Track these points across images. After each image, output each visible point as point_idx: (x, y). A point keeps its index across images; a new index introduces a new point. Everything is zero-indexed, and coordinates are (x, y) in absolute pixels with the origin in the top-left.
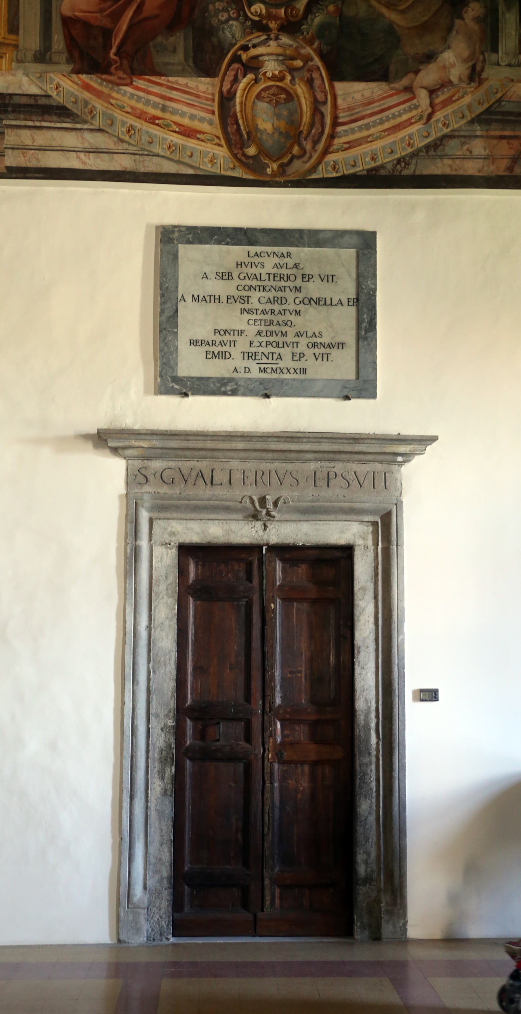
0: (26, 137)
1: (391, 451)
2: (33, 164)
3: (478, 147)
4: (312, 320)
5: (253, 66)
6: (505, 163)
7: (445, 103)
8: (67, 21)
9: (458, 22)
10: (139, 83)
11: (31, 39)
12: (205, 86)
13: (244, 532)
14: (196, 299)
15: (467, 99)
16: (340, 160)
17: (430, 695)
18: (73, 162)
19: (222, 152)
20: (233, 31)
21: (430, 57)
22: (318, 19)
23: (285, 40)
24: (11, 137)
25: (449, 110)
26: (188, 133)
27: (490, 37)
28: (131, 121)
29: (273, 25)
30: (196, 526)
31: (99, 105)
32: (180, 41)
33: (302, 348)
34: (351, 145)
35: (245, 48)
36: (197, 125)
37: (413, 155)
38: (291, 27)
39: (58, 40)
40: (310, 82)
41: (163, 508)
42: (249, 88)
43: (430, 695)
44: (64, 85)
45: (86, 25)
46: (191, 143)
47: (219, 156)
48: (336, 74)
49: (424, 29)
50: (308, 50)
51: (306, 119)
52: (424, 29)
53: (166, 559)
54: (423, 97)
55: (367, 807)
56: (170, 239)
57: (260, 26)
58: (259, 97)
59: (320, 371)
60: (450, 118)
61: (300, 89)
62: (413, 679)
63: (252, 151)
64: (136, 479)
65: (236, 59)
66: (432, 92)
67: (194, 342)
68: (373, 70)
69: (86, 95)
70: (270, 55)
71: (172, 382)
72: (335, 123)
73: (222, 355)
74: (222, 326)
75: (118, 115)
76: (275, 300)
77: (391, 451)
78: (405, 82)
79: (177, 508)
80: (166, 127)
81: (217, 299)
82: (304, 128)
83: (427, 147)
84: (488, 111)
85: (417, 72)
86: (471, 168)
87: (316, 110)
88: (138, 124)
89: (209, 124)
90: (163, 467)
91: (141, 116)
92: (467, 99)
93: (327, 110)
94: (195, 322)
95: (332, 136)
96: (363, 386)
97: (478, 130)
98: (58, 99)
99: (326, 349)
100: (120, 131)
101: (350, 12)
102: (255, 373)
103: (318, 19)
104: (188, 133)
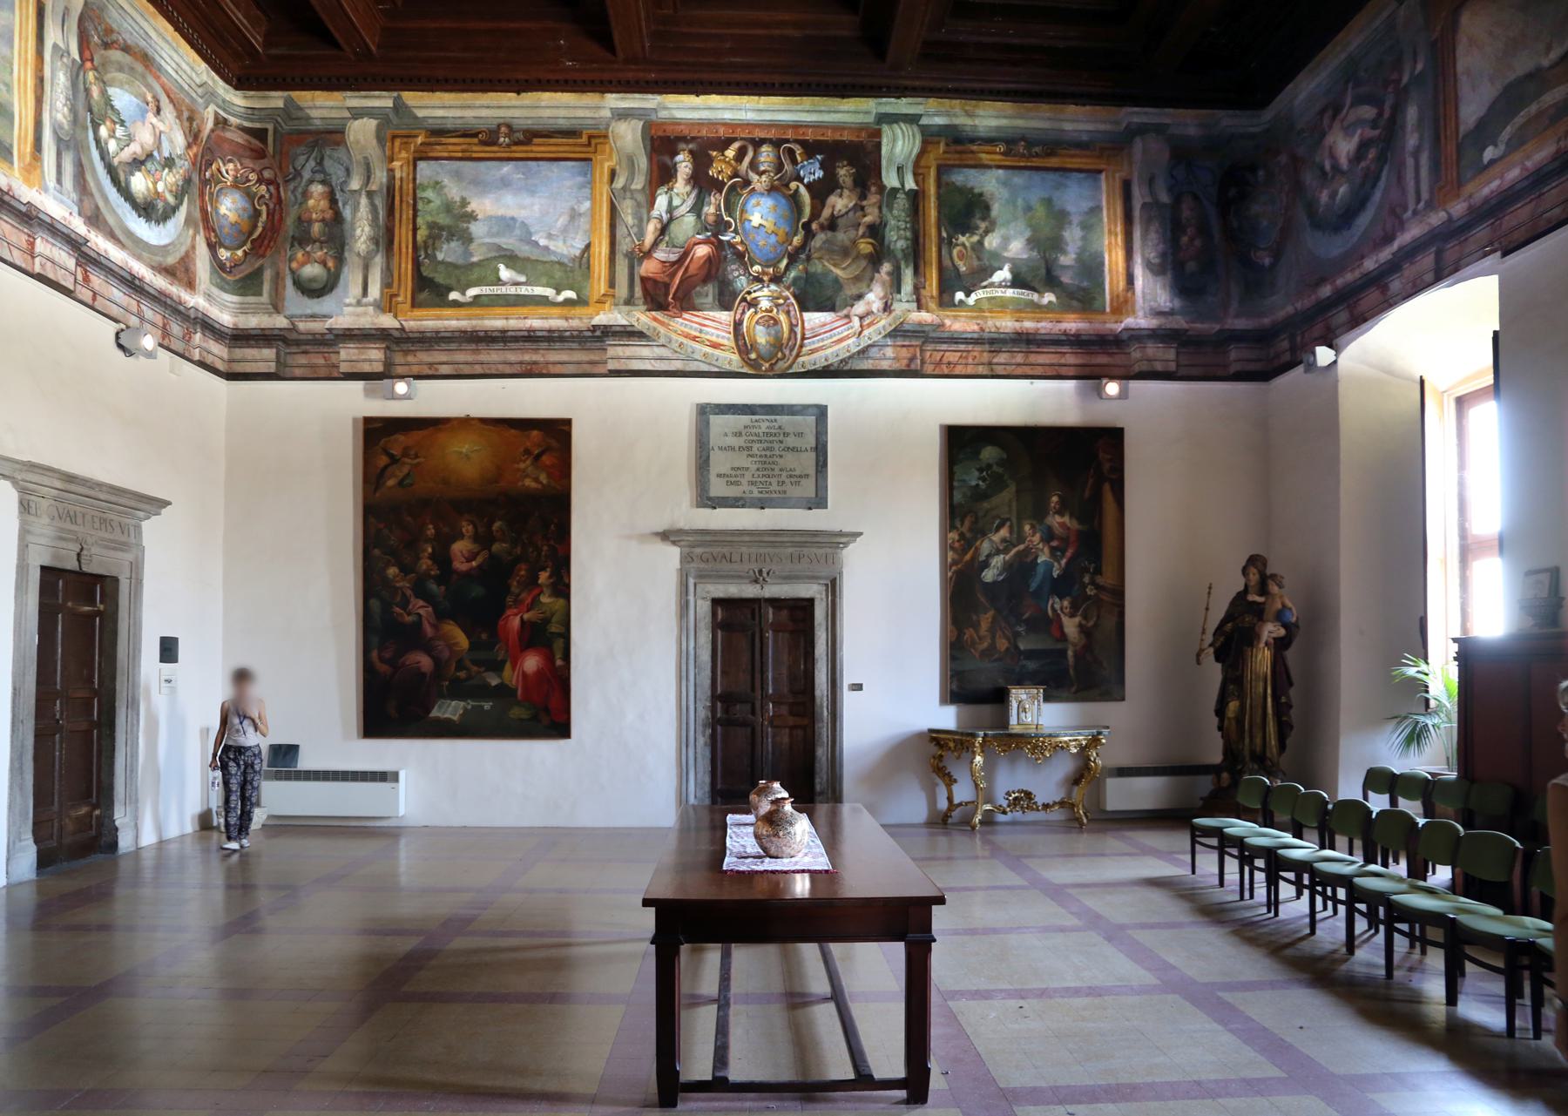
0: (620, 351)
1: (835, 541)
2: (623, 367)
3: (889, 352)
4: (789, 460)
5: (753, 304)
6: (905, 362)
7: (869, 325)
8: (644, 280)
10: (685, 315)
11: (622, 290)
12: (726, 317)
13: (750, 591)
14: (720, 448)
15: (883, 322)
16: (807, 361)
18: (647, 366)
19: (736, 357)
20: (742, 282)
21: (860, 297)
22: (793, 274)
23: (773, 287)
24: (611, 352)
25: (871, 329)
26: (715, 346)
27: (896, 284)
30: (721, 587)
31: (662, 330)
32: (710, 289)
33: (783, 478)
34: (813, 351)
38: (776, 279)
40: (788, 313)
41: (702, 576)
42: (752, 317)
44: (641, 318)
45: (655, 281)
46: (717, 352)
47: (732, 360)
49: (857, 279)
50: (787, 293)
51: (786, 335)
52: (857, 279)
54: (856, 321)
57: (758, 279)
59: (794, 492)
60: (872, 334)
61: (782, 317)
63: (753, 356)
64: (686, 559)
65: (744, 299)
66: (861, 318)
67: (719, 476)
68: (826, 304)
69: (655, 324)
70: (764, 296)
71: (706, 500)
72: (803, 338)
73: (737, 483)
74: (736, 465)
75: (674, 336)
77: (835, 541)
78: (845, 312)
79: (710, 576)
81: (733, 449)
86: (885, 365)
87: (792, 327)
88: (685, 341)
89: (727, 339)
90: (702, 552)
91: (687, 336)
92: (883, 322)
93: (798, 330)
95: (801, 346)
96: (819, 501)
98: (638, 327)
99: (799, 478)
100: (675, 346)
101: (812, 269)
102: (756, 494)
103: (793, 274)
104: (715, 346)
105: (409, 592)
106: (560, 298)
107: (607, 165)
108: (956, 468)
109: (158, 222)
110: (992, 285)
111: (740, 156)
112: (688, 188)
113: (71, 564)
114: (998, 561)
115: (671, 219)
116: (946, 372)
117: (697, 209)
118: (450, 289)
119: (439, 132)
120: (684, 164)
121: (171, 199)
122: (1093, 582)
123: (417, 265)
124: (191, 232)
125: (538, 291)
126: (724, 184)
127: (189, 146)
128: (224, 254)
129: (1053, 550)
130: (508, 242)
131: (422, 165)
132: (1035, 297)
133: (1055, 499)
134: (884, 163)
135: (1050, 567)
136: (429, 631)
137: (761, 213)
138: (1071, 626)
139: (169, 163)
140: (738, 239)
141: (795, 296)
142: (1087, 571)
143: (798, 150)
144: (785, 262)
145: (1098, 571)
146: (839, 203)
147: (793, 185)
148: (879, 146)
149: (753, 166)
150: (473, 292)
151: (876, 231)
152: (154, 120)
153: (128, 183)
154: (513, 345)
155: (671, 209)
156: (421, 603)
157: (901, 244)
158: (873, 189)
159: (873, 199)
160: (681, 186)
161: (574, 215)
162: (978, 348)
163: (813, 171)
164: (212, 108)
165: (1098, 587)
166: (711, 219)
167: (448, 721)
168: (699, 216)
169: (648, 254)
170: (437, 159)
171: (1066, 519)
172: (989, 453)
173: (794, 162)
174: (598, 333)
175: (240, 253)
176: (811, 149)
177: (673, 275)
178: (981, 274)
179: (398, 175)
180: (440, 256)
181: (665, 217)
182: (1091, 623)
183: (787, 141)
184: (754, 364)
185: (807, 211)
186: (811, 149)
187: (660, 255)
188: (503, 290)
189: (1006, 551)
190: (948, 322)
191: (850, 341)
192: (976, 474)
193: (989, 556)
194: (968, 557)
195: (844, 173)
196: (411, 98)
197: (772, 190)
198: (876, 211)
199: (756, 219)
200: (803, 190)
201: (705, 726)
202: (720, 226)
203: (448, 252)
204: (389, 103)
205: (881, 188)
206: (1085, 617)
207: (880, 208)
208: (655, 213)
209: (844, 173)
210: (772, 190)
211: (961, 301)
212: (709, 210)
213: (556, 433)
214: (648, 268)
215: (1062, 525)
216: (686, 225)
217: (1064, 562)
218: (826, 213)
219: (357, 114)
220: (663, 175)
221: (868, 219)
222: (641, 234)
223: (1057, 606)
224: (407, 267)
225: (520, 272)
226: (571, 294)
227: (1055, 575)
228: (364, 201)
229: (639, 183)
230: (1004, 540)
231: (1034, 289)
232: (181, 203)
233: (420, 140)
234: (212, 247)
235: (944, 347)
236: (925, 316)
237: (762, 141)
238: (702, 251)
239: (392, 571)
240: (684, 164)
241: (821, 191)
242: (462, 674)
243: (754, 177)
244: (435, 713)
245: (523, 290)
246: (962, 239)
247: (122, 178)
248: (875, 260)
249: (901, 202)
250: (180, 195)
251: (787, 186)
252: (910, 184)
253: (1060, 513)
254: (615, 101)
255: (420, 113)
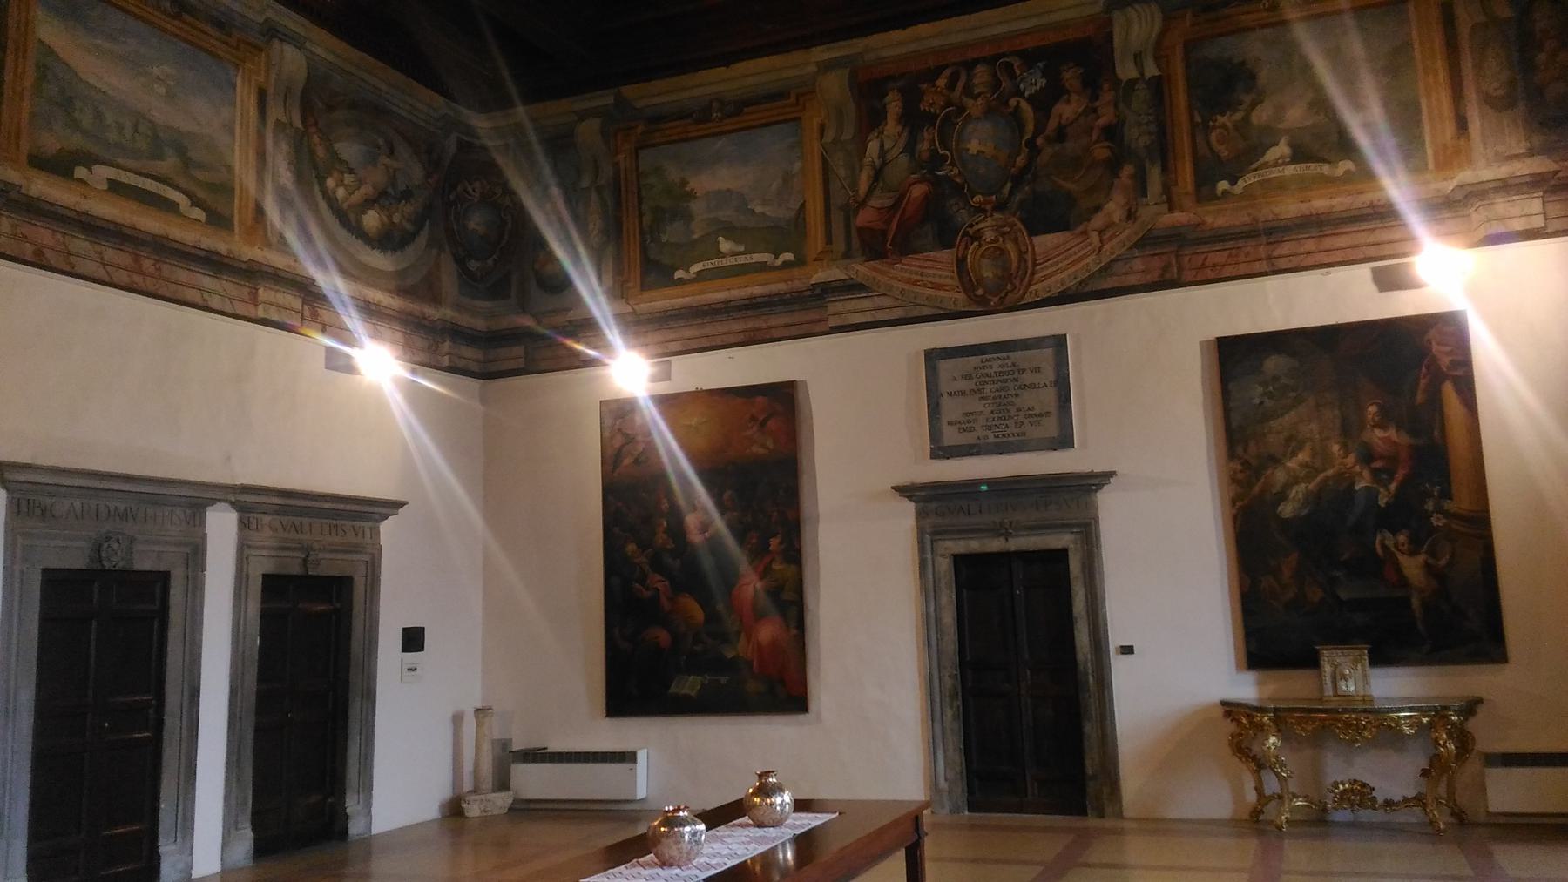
0: (839, 306)
1: (1087, 485)
4: (1027, 399)
5: (977, 237)
7: (1110, 239)
8: (860, 230)
9: (1116, 181)
11: (839, 245)
12: (946, 255)
14: (950, 394)
15: (1127, 232)
16: (1039, 289)
17: (1127, 650)
19: (961, 296)
20: (963, 216)
21: (1098, 209)
23: (997, 215)
24: (832, 308)
25: (1115, 241)
26: (937, 287)
27: (1141, 186)
28: (901, 285)
29: (989, 207)
30: (962, 543)
31: (880, 277)
33: (1021, 419)
34: (1046, 277)
35: (971, 226)
36: (942, 281)
37: (1091, 276)
38: (1000, 207)
39: (856, 243)
40: (1016, 241)
41: (939, 533)
42: (976, 251)
43: (1127, 650)
44: (861, 270)
46: (941, 293)
47: (958, 298)
48: (1033, 232)
51: (1015, 265)
53: (945, 565)
54: (1095, 237)
55: (1089, 728)
56: (933, 357)
57: (980, 210)
58: (983, 256)
59: (1035, 433)
61: (1010, 246)
62: (1115, 640)
63: (980, 292)
64: (921, 515)
66: (1101, 232)
67: (950, 423)
68: (1059, 224)
70: (987, 227)
71: (941, 452)
72: (1035, 264)
73: (972, 430)
74: (968, 409)
75: (895, 283)
76: (1002, 389)
77: (1087, 485)
78: (1081, 228)
79: (946, 532)
80: (925, 285)
81: (963, 393)
82: (1013, 270)
83: (1100, 270)
84: (1142, 238)
85: (1089, 220)
86: (1132, 280)
87: (1022, 259)
88: (906, 287)
90: (934, 503)
93: (1029, 257)
94: (952, 409)
95: (1033, 274)
96: (1064, 441)
97: (1136, 252)
99: (1037, 417)
102: (992, 439)
104: (937, 287)
105: (647, 568)
106: (779, 262)
107: (816, 122)
108: (1231, 386)
109: (394, 250)
110: (1266, 165)
111: (951, 85)
112: (899, 128)
113: (296, 570)
114: (1298, 491)
115: (884, 164)
116: (1211, 275)
117: (910, 148)
118: (674, 269)
119: (657, 119)
120: (894, 104)
121: (408, 226)
122: (1440, 510)
123: (644, 251)
124: (434, 251)
125: (757, 258)
126: (936, 116)
127: (428, 175)
128: (473, 265)
129: (1375, 473)
130: (725, 214)
131: (643, 153)
132: (1326, 169)
133: (1372, 409)
134: (1117, 55)
135: (1371, 494)
136: (666, 605)
137: (979, 140)
138: (1412, 567)
139: (407, 195)
140: (955, 171)
141: (1021, 220)
142: (1430, 495)
143: (1016, 62)
144: (1009, 185)
145: (1447, 494)
146: (1066, 110)
147: (1013, 102)
148: (1110, 37)
149: (968, 91)
150: (695, 268)
151: (1112, 133)
152: (387, 161)
153: (359, 221)
154: (735, 315)
155: (883, 153)
156: (658, 577)
157: (1144, 141)
158: (1106, 86)
159: (1107, 96)
160: (891, 127)
161: (787, 178)
162: (1252, 242)
163: (1035, 82)
164: (454, 137)
165: (1446, 514)
166: (925, 156)
167: (686, 696)
168: (912, 155)
169: (863, 204)
170: (654, 145)
171: (1391, 433)
172: (1274, 364)
173: (1013, 76)
174: (818, 291)
175: (490, 262)
176: (1029, 58)
177: (888, 222)
178: (1249, 154)
179: (622, 167)
180: (664, 238)
181: (878, 162)
182: (1443, 562)
183: (1004, 55)
184: (982, 301)
185: (1030, 127)
186: (1029, 58)
187: (875, 202)
188: (724, 262)
189: (1308, 478)
190: (1209, 219)
191: (1088, 260)
192: (1260, 389)
193: (1288, 486)
194: (1256, 489)
195: (1070, 76)
196: (628, 91)
197: (989, 112)
198: (1112, 110)
199: (974, 146)
200: (1024, 105)
201: (953, 696)
202: (936, 160)
203: (672, 233)
204: (611, 100)
205: (1116, 82)
206: (1433, 553)
207: (1116, 106)
208: (867, 160)
209: (1070, 76)
210: (989, 112)
211: (1225, 192)
212: (924, 147)
213: (780, 404)
214: (864, 218)
215: (1387, 440)
216: (900, 165)
217: (1393, 487)
218: (1052, 124)
219: (583, 116)
220: (872, 120)
221: (1102, 121)
222: (854, 185)
223: (1390, 543)
224: (636, 255)
225: (737, 241)
226: (789, 256)
227: (1382, 502)
228: (594, 196)
229: (848, 135)
230: (1304, 465)
231: (1324, 161)
232: (421, 227)
233: (640, 129)
234: (460, 261)
235: (1205, 248)
236: (1179, 217)
237: (976, 62)
238: (918, 191)
239: (631, 547)
240: (894, 105)
241: (1043, 103)
242: (698, 648)
243: (969, 102)
244: (673, 689)
245: (742, 260)
246: (1221, 119)
247: (352, 217)
248: (1113, 166)
249: (1142, 94)
250: (419, 223)
251: (1006, 104)
252: (1151, 70)
253: (1381, 426)
254: (821, 53)
255: (639, 104)
